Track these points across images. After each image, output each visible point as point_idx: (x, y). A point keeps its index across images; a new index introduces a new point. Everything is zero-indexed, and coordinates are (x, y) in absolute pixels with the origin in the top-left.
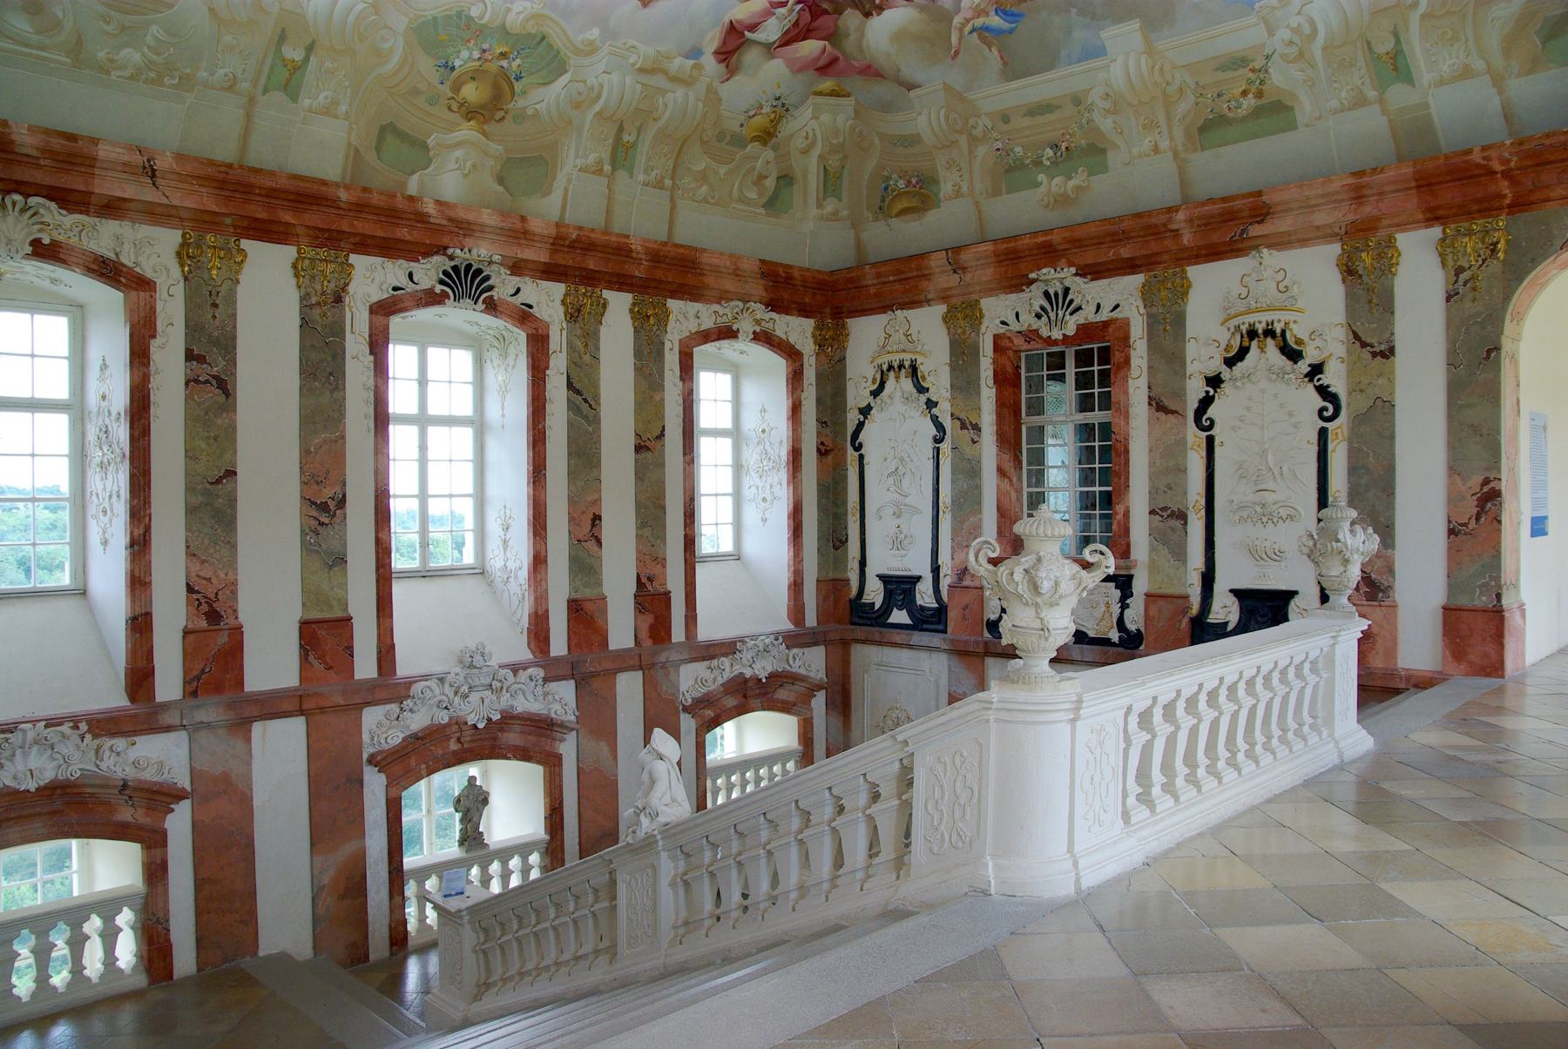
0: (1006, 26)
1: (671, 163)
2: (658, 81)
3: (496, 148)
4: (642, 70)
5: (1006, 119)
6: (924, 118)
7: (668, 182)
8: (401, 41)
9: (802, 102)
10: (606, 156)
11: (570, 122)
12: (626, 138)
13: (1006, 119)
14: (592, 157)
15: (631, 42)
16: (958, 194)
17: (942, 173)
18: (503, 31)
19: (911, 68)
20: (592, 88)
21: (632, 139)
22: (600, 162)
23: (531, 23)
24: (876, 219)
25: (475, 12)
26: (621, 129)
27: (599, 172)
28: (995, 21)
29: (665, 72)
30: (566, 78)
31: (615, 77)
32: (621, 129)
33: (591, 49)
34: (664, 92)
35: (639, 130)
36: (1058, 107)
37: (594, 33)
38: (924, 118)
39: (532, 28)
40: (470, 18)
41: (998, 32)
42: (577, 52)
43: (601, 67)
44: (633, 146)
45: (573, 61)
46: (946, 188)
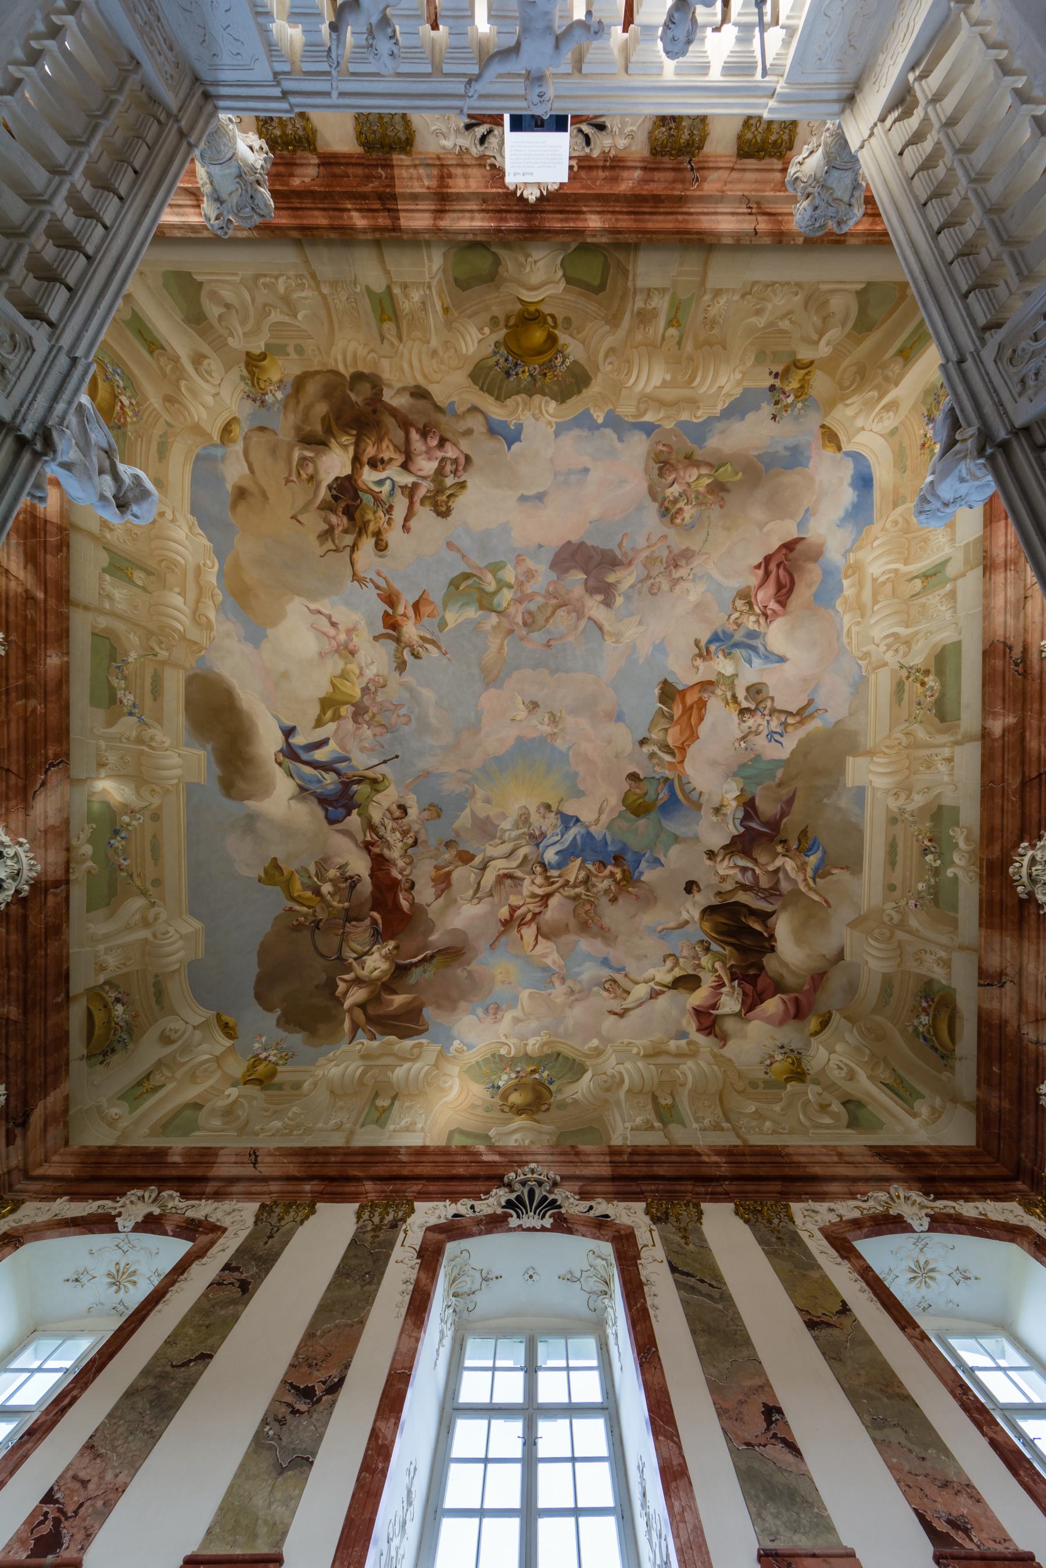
0: (819, 854)
1: (719, 1111)
2: (663, 1060)
3: (551, 1128)
4: (646, 1056)
5: (892, 888)
6: (872, 961)
7: (725, 1125)
8: (457, 1080)
9: (808, 1045)
10: (652, 1116)
11: (606, 1101)
12: (663, 1102)
13: (892, 888)
14: (639, 1120)
15: (626, 1041)
16: (947, 964)
17: (923, 971)
18: (528, 1058)
19: (827, 946)
20: (613, 1076)
21: (669, 1101)
22: (648, 1121)
23: (545, 1049)
24: (952, 1069)
25: (503, 1051)
26: (655, 1098)
27: (652, 1128)
28: (813, 860)
29: (667, 1053)
30: (588, 1075)
31: (628, 1065)
32: (655, 1098)
33: (598, 1052)
34: (677, 1066)
35: (672, 1094)
36: (894, 839)
37: (595, 1042)
38: (872, 961)
39: (546, 1050)
40: (501, 1056)
41: (822, 860)
42: (588, 1056)
43: (613, 1060)
44: (672, 1107)
45: (588, 1063)
46: (938, 974)
